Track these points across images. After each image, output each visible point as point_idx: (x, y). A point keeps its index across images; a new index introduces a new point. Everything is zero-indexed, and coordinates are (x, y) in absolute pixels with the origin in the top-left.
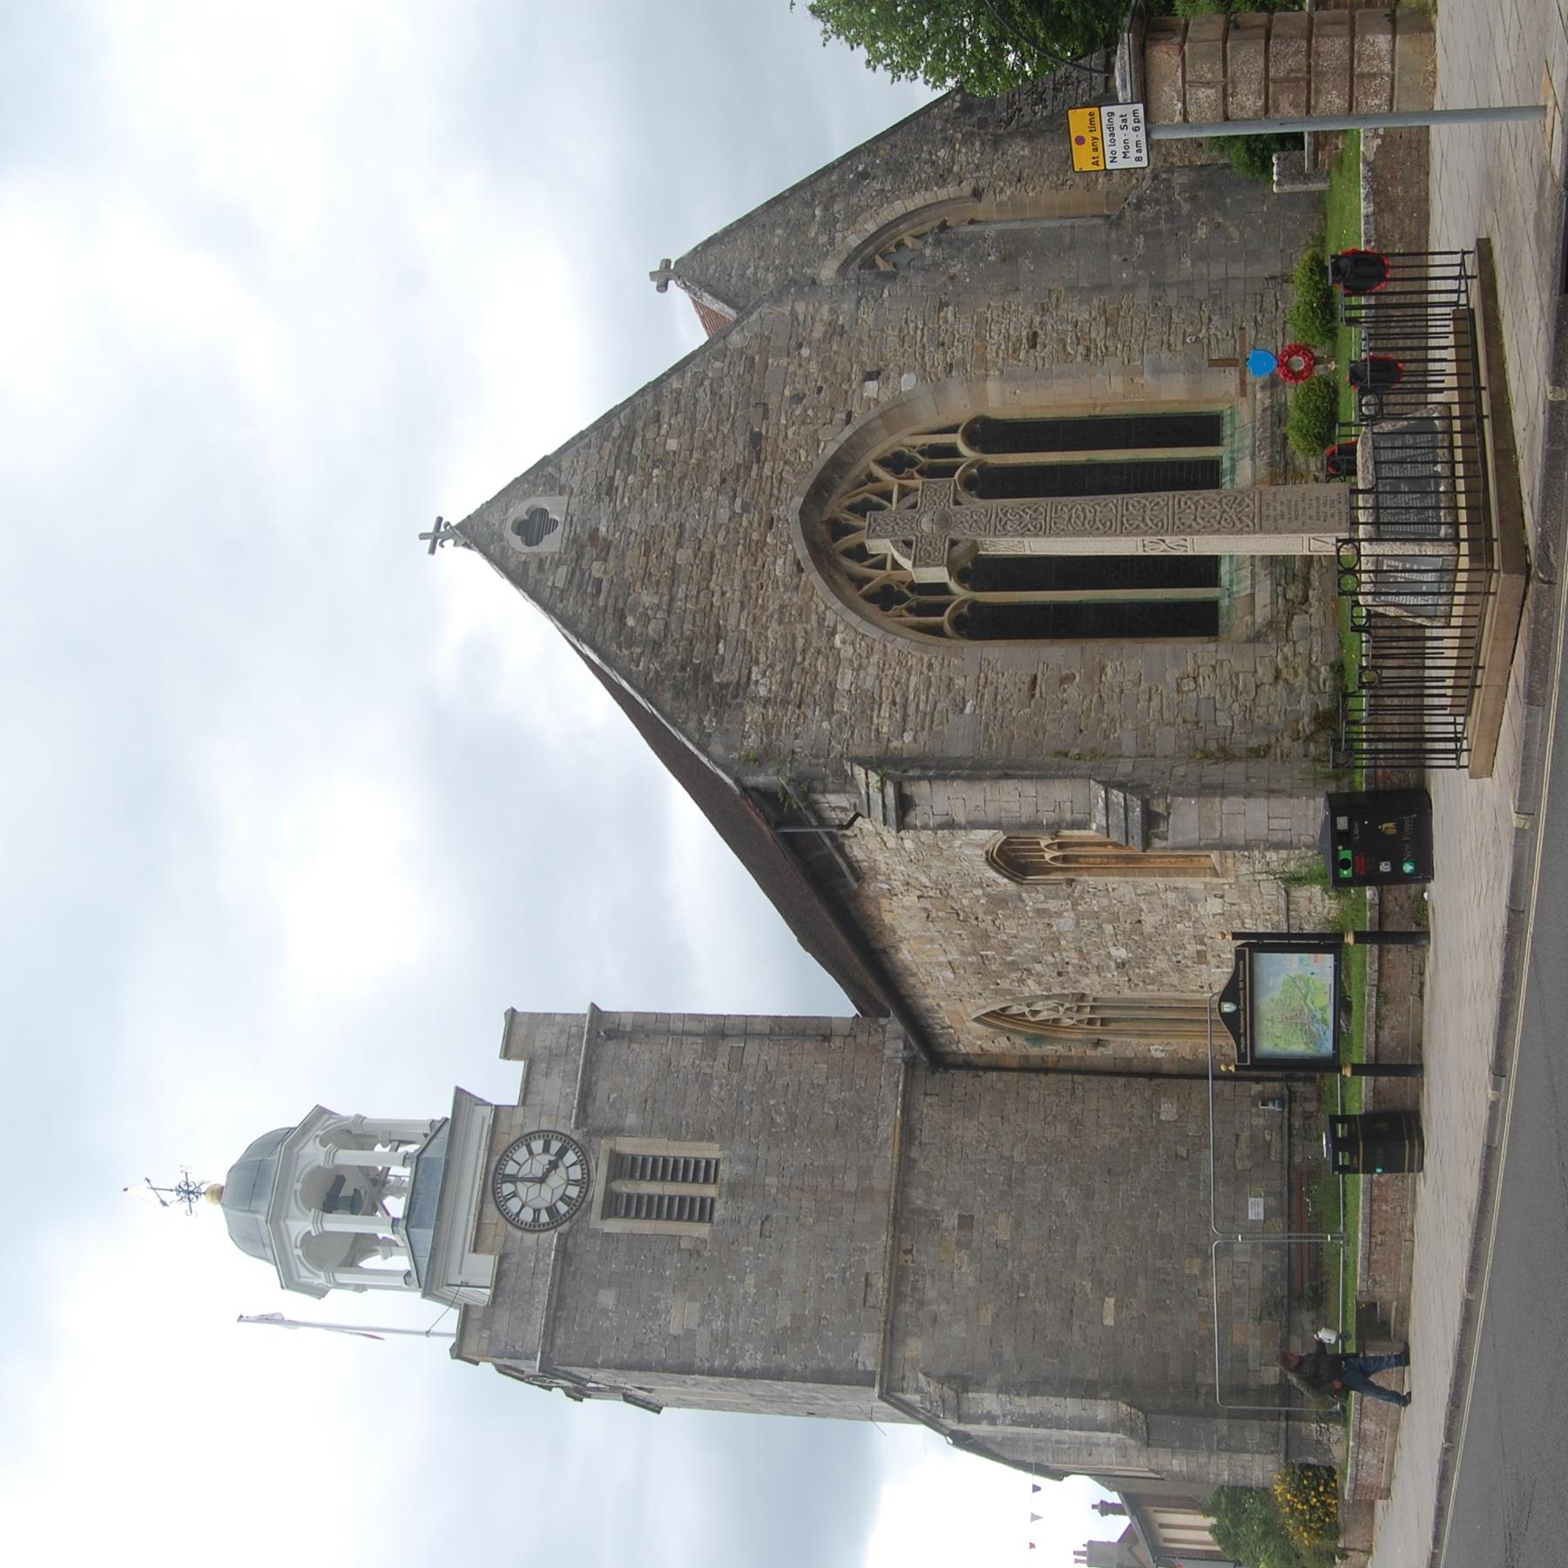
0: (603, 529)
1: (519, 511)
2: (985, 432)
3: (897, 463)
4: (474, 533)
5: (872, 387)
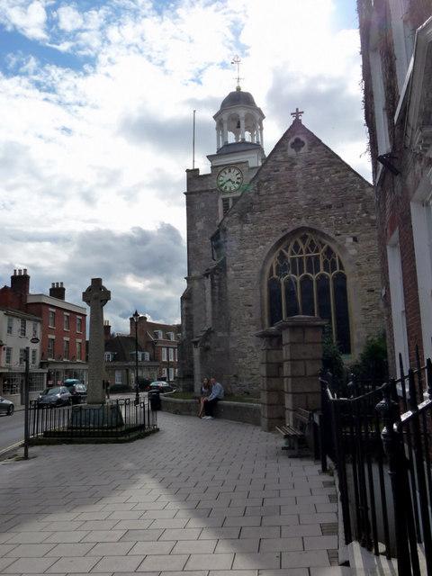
0: (295, 167)
1: (303, 138)
2: (341, 280)
3: (329, 252)
4: (297, 125)
5: (351, 240)
